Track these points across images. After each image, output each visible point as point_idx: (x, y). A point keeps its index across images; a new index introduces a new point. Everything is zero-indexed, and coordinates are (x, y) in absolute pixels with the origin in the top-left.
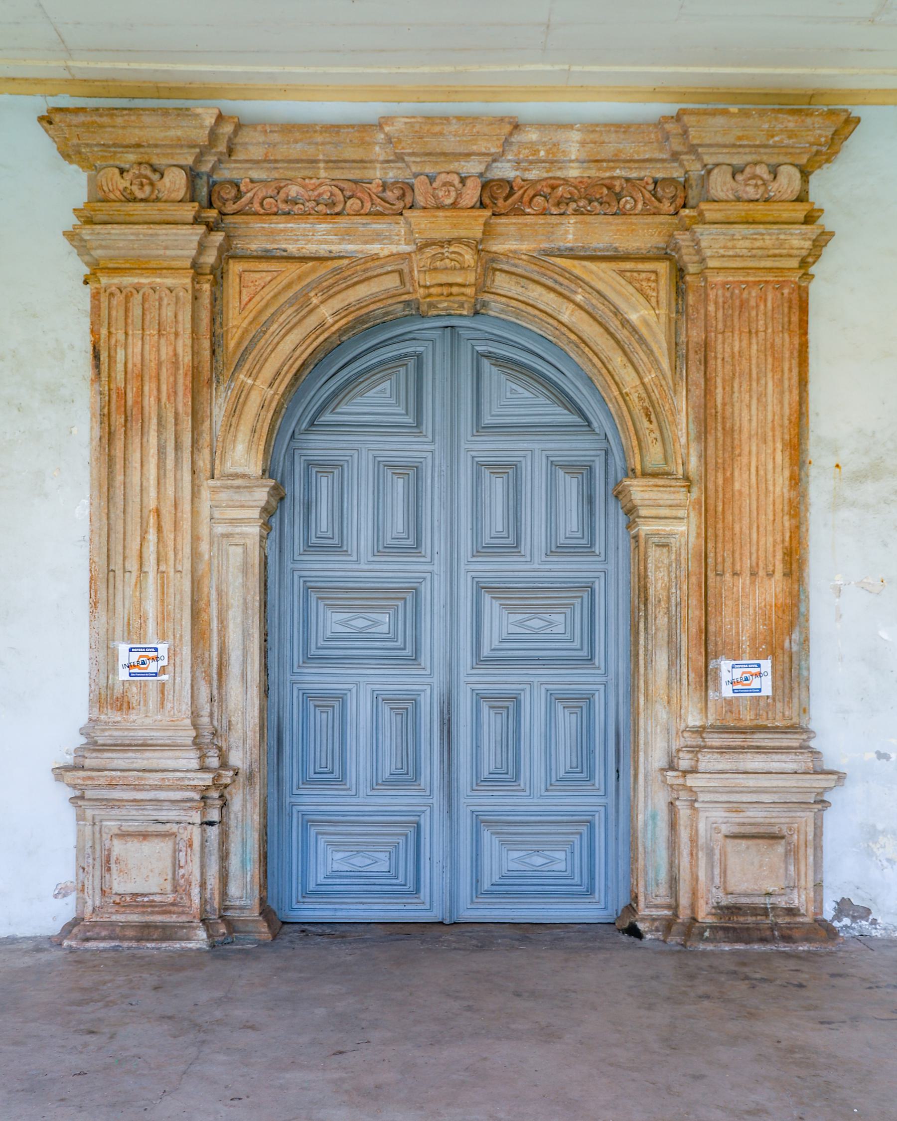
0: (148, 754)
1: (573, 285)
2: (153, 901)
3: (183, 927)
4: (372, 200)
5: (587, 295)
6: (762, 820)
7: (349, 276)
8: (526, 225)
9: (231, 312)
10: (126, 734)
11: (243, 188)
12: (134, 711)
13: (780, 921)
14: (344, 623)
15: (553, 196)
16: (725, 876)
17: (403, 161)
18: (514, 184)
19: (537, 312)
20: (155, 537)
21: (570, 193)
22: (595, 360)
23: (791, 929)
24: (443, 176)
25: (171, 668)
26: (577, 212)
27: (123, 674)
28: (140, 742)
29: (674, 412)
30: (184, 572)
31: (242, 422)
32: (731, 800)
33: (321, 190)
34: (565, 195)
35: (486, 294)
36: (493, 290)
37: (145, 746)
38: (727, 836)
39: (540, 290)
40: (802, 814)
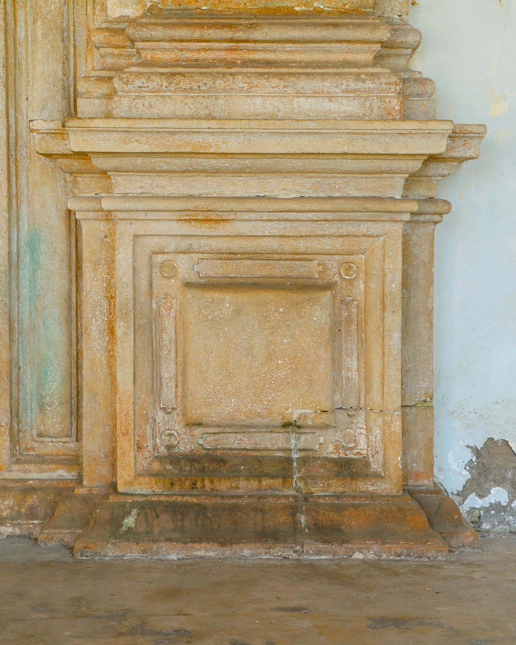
6: (274, 244)
13: (317, 489)
16: (184, 383)
23: (339, 509)
32: (195, 192)
38: (188, 285)
40: (373, 228)
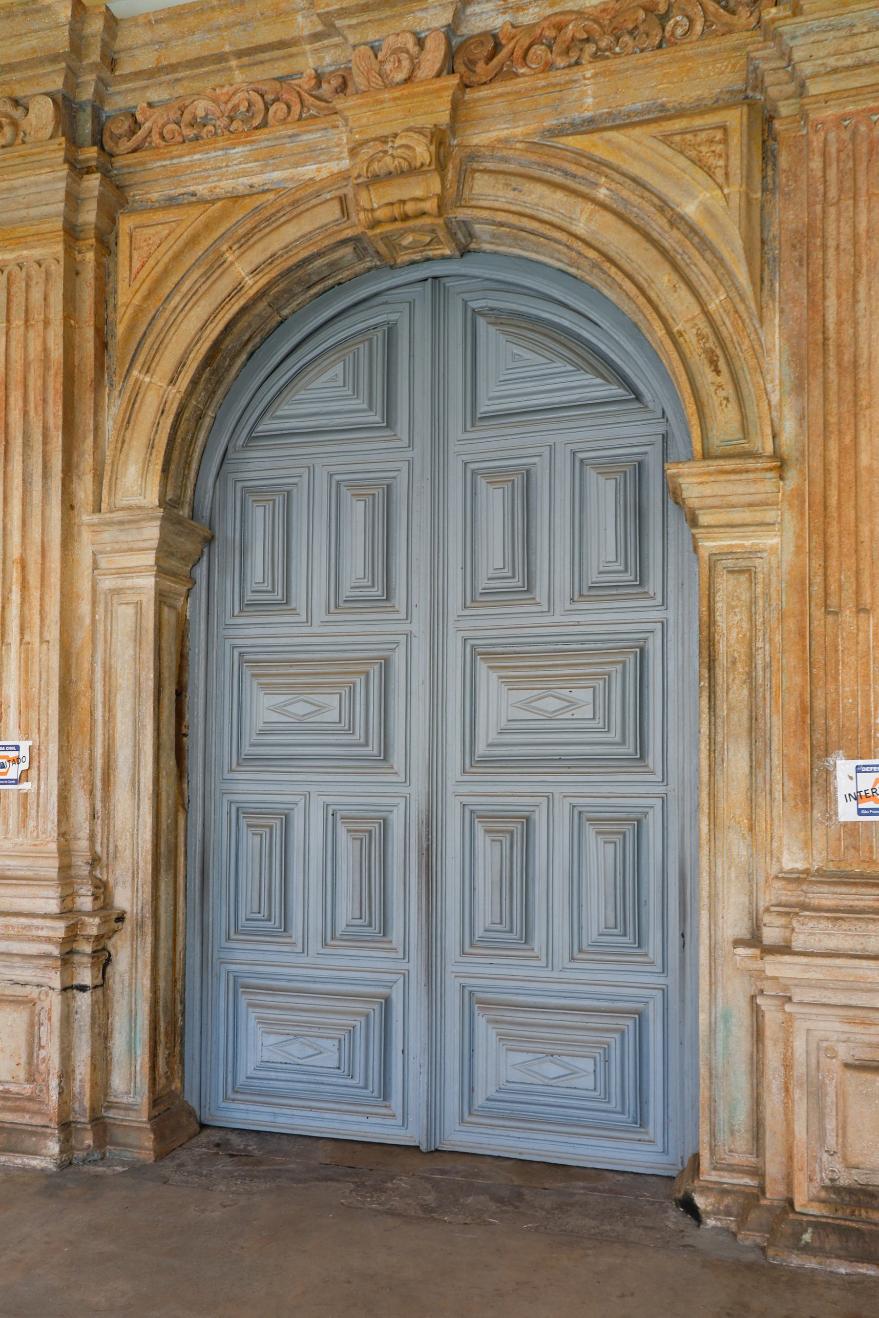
1: (592, 174)
4: (302, 102)
5: (613, 186)
7: (273, 215)
11: (139, 118)
14: (275, 709)
15: (558, 40)
17: (338, 32)
18: (501, 36)
19: (534, 225)
21: (587, 32)
22: (627, 285)
24: (391, 39)
26: (596, 57)
29: (758, 352)
33: (235, 100)
34: (578, 35)
35: (460, 210)
36: (473, 203)
39: (540, 189)
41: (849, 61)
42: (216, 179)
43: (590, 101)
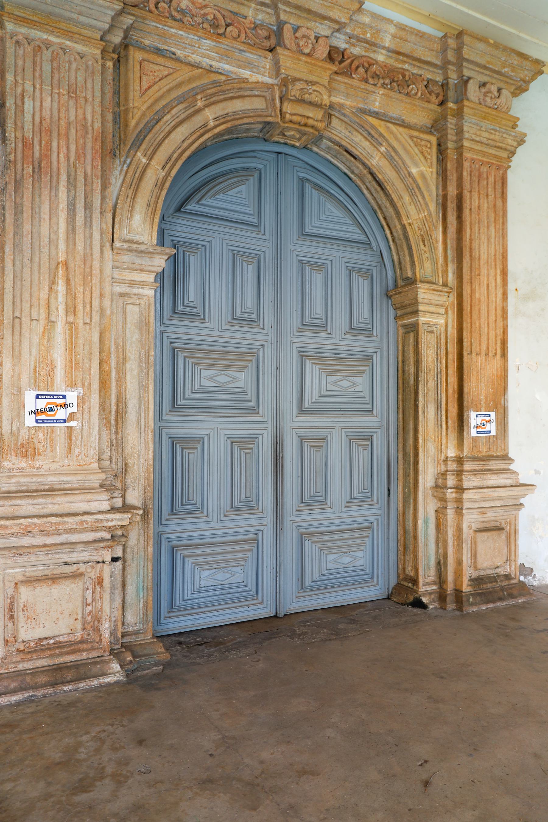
0: (59, 499)
2: (59, 642)
3: (96, 663)
7: (228, 90)
8: (351, 86)
9: (131, 94)
10: (34, 479)
12: (40, 457)
20: (64, 288)
25: (79, 415)
26: (384, 86)
27: (30, 421)
28: (47, 487)
30: (93, 325)
31: (139, 194)
33: (207, 10)
37: (52, 491)
41: (478, 139)
42: (190, 51)
43: (377, 104)
